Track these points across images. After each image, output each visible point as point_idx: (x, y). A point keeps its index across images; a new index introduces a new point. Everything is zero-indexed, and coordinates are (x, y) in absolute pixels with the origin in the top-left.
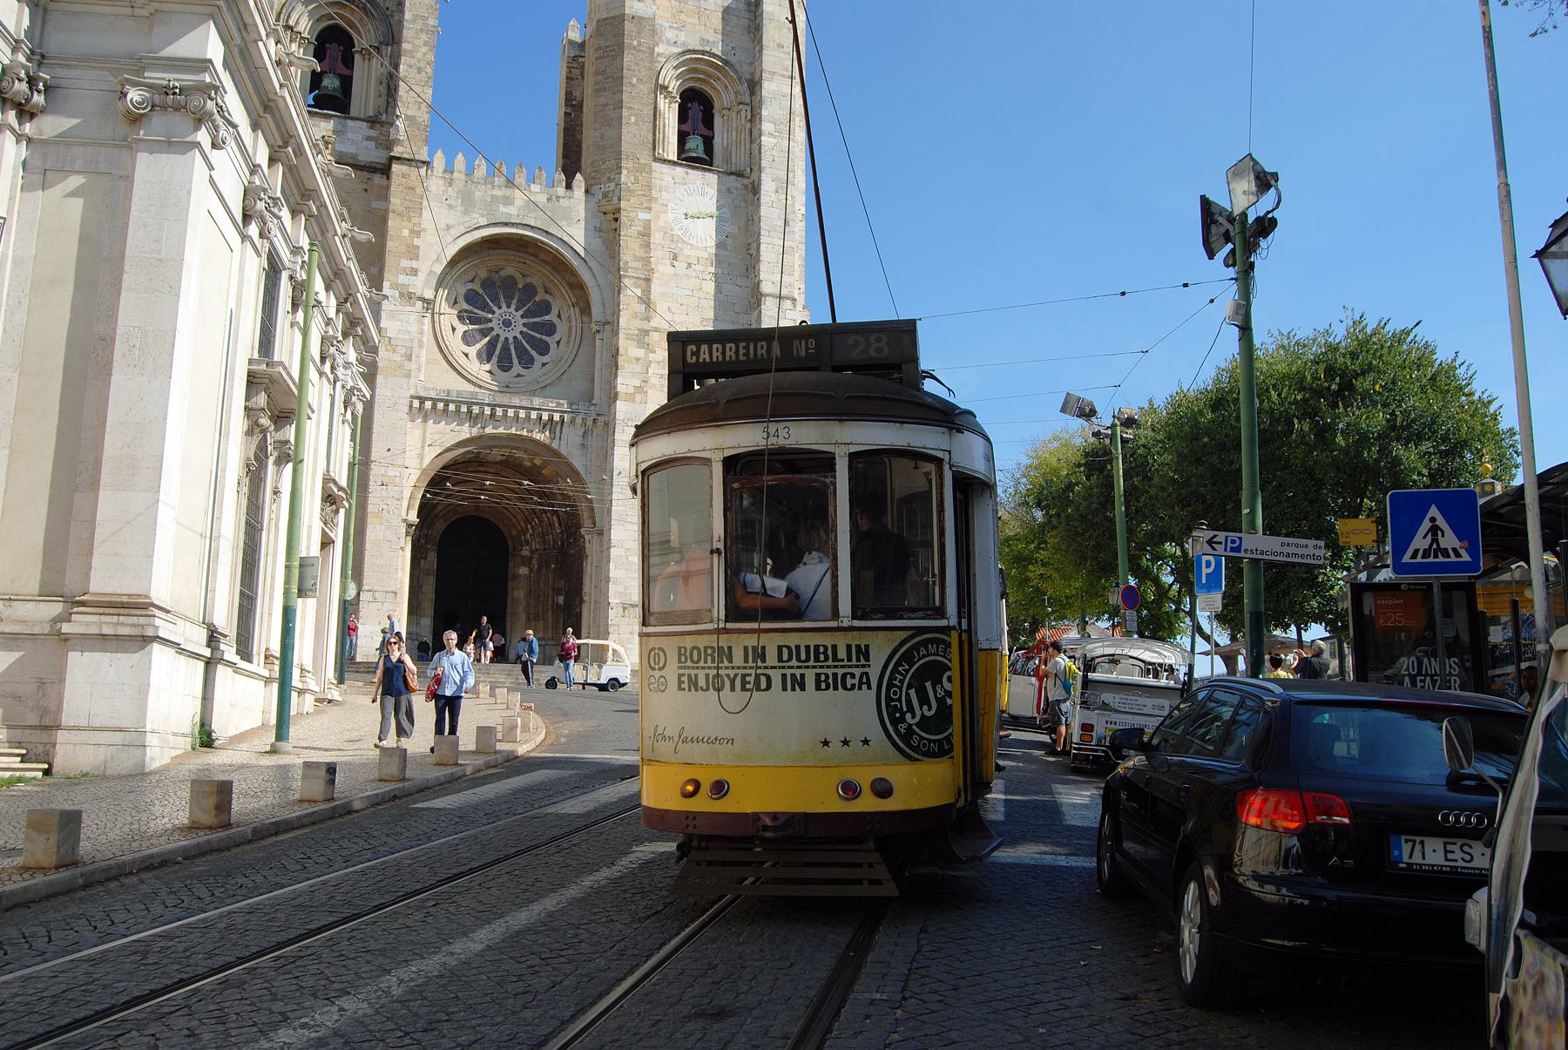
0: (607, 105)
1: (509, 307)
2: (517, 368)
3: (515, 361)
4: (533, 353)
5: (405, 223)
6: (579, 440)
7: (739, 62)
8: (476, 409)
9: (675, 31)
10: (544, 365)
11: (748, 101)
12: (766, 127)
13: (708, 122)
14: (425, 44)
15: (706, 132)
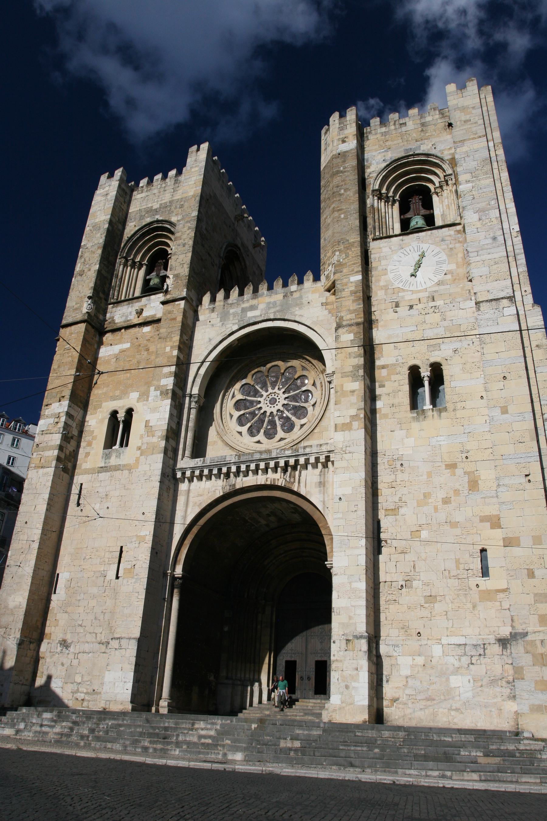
0: (327, 216)
1: (273, 389)
2: (280, 434)
3: (279, 428)
4: (293, 418)
5: (168, 343)
6: (316, 479)
7: (440, 151)
8: (224, 470)
9: (383, 154)
10: (302, 426)
11: (449, 171)
12: (462, 178)
13: (428, 204)
14: (189, 228)
15: (427, 212)
